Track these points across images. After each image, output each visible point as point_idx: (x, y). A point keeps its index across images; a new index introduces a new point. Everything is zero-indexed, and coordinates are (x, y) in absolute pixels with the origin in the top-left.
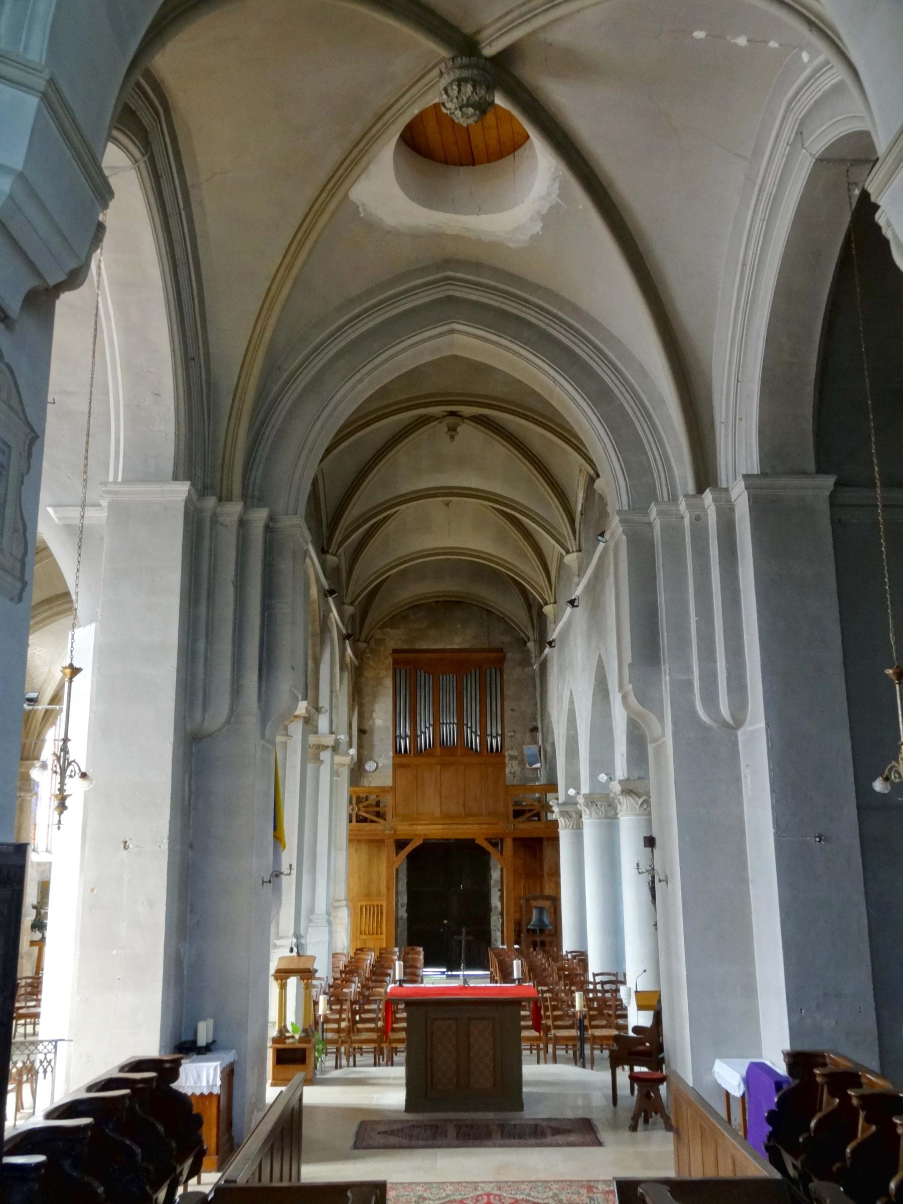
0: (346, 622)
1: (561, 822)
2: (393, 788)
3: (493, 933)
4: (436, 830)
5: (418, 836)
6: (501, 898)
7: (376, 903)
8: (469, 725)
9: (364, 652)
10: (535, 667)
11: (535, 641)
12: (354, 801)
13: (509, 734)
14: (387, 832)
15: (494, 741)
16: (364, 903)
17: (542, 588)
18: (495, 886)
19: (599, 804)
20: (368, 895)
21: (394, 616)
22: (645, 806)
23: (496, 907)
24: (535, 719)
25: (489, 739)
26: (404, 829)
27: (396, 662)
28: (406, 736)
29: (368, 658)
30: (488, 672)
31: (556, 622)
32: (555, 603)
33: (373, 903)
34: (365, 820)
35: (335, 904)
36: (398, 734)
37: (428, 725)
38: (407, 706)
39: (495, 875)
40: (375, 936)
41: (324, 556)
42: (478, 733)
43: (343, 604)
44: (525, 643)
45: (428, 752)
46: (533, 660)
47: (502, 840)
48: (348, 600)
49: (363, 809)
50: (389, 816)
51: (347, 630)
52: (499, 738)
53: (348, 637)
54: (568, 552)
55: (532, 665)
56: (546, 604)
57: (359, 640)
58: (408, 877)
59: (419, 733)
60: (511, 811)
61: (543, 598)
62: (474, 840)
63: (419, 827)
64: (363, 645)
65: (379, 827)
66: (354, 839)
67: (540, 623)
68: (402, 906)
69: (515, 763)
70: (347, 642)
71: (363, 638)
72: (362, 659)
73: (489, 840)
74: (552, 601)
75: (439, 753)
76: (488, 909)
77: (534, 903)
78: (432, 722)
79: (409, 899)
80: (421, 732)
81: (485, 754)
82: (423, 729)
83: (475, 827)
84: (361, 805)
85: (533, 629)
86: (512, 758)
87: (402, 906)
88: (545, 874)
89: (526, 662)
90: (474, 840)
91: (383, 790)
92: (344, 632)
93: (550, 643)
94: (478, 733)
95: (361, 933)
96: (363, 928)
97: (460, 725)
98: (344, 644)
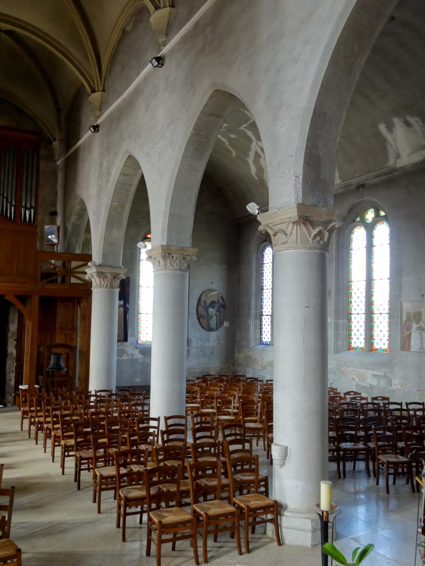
1: (96, 281)
3: (7, 375)
8: (5, 195)
10: (58, 163)
11: (61, 140)
18: (11, 337)
19: (175, 256)
22: (318, 239)
23: (12, 354)
24: (55, 206)
32: (104, 91)
39: (13, 328)
42: (13, 202)
46: (57, 157)
54: (157, 8)
55: (55, 161)
56: (93, 91)
60: (39, 274)
73: (17, 297)
74: (101, 88)
76: (4, 355)
77: (54, 350)
83: (5, 284)
88: (57, 327)
93: (96, 128)
94: (13, 202)
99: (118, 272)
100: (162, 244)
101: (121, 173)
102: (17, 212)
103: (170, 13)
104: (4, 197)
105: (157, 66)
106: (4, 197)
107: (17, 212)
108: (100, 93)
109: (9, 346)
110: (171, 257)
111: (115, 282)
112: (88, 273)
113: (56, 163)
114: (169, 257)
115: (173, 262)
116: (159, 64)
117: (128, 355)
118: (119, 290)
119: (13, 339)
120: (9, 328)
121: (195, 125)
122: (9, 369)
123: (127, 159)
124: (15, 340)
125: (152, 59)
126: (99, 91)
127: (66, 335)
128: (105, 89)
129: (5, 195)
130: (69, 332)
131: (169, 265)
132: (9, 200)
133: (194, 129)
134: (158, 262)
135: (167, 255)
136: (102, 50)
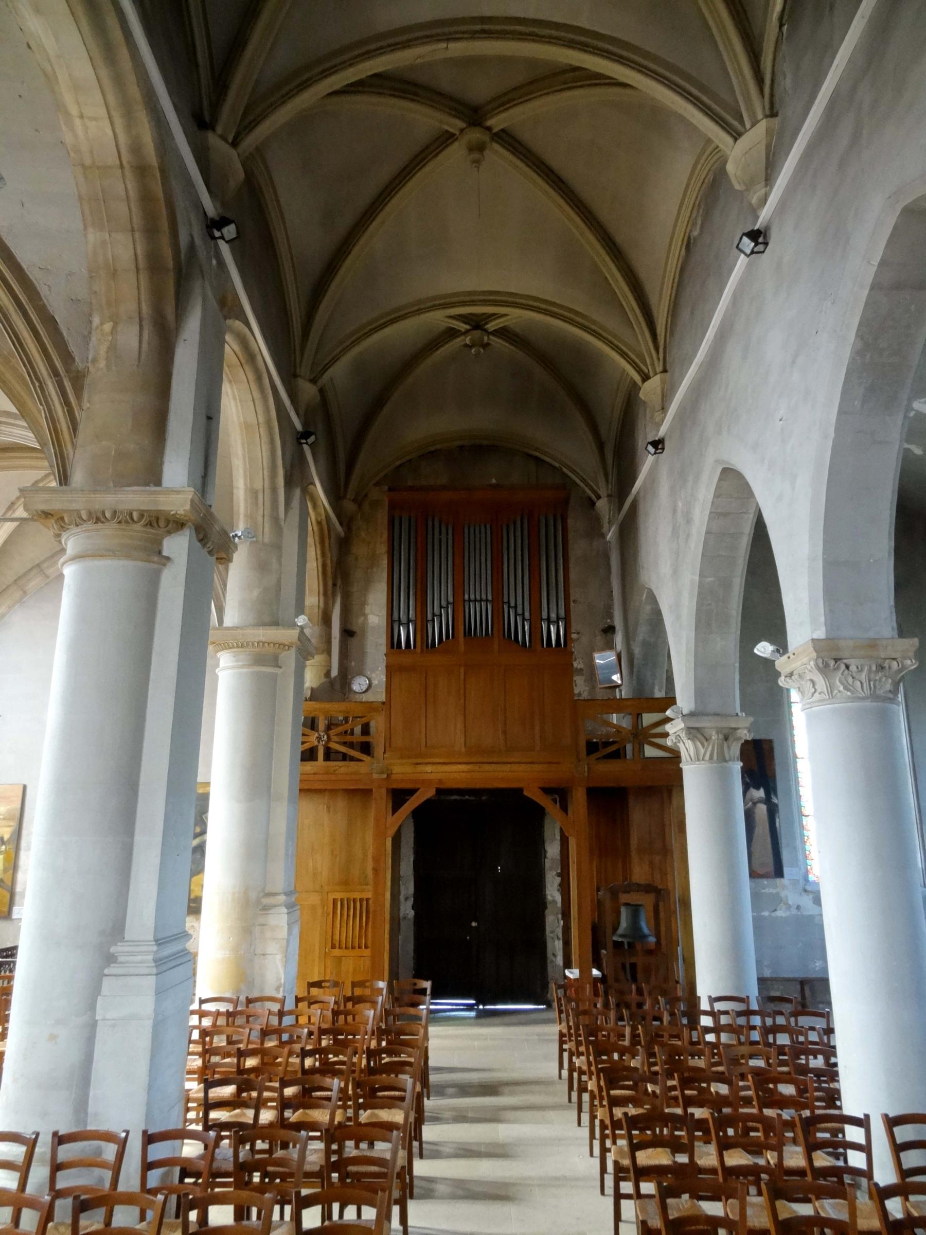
0: (302, 412)
1: (687, 749)
2: (387, 704)
4: (456, 773)
5: (427, 783)
6: (564, 888)
7: (358, 896)
8: (512, 604)
10: (608, 537)
11: (609, 496)
12: (322, 725)
14: (375, 776)
15: (553, 629)
16: (338, 896)
17: (640, 356)
18: (551, 869)
20: (345, 883)
23: (555, 902)
24: (610, 616)
25: (544, 625)
26: (403, 771)
28: (409, 621)
31: (664, 409)
32: (665, 371)
33: (353, 895)
34: (345, 757)
35: (266, 901)
36: (396, 617)
38: (412, 582)
39: (553, 850)
40: (357, 952)
42: (527, 615)
43: (295, 376)
44: (593, 504)
45: (446, 644)
49: (335, 739)
50: (379, 750)
53: (305, 435)
55: (603, 536)
56: (646, 378)
58: (416, 853)
59: (429, 617)
61: (639, 371)
62: (519, 791)
63: (429, 769)
68: (406, 899)
71: (350, 494)
73: (547, 791)
74: (659, 368)
75: (462, 648)
76: (541, 904)
77: (624, 898)
78: (451, 599)
80: (434, 615)
83: (523, 767)
84: (332, 733)
85: (606, 475)
87: (406, 899)
91: (371, 707)
92: (299, 426)
93: (658, 444)
94: (527, 615)
95: (333, 947)
96: (337, 937)
97: (498, 601)
99: (734, 726)
100: (815, 637)
101: (711, 513)
102: (535, 630)
103: (769, 132)
104: (509, 607)
105: (752, 252)
107: (535, 630)
108: (658, 377)
110: (843, 667)
111: (729, 748)
112: (671, 732)
114: (836, 669)
115: (850, 680)
116: (757, 244)
117: (789, 907)
118: (742, 764)
120: (545, 852)
121: (860, 325)
122: (552, 932)
123: (720, 479)
124: (559, 875)
125: (741, 239)
126: (656, 374)
127: (651, 863)
128: (668, 367)
130: (657, 859)
131: (841, 688)
132: (520, 611)
133: (860, 335)
134: (809, 684)
135: (832, 663)
136: (653, 300)
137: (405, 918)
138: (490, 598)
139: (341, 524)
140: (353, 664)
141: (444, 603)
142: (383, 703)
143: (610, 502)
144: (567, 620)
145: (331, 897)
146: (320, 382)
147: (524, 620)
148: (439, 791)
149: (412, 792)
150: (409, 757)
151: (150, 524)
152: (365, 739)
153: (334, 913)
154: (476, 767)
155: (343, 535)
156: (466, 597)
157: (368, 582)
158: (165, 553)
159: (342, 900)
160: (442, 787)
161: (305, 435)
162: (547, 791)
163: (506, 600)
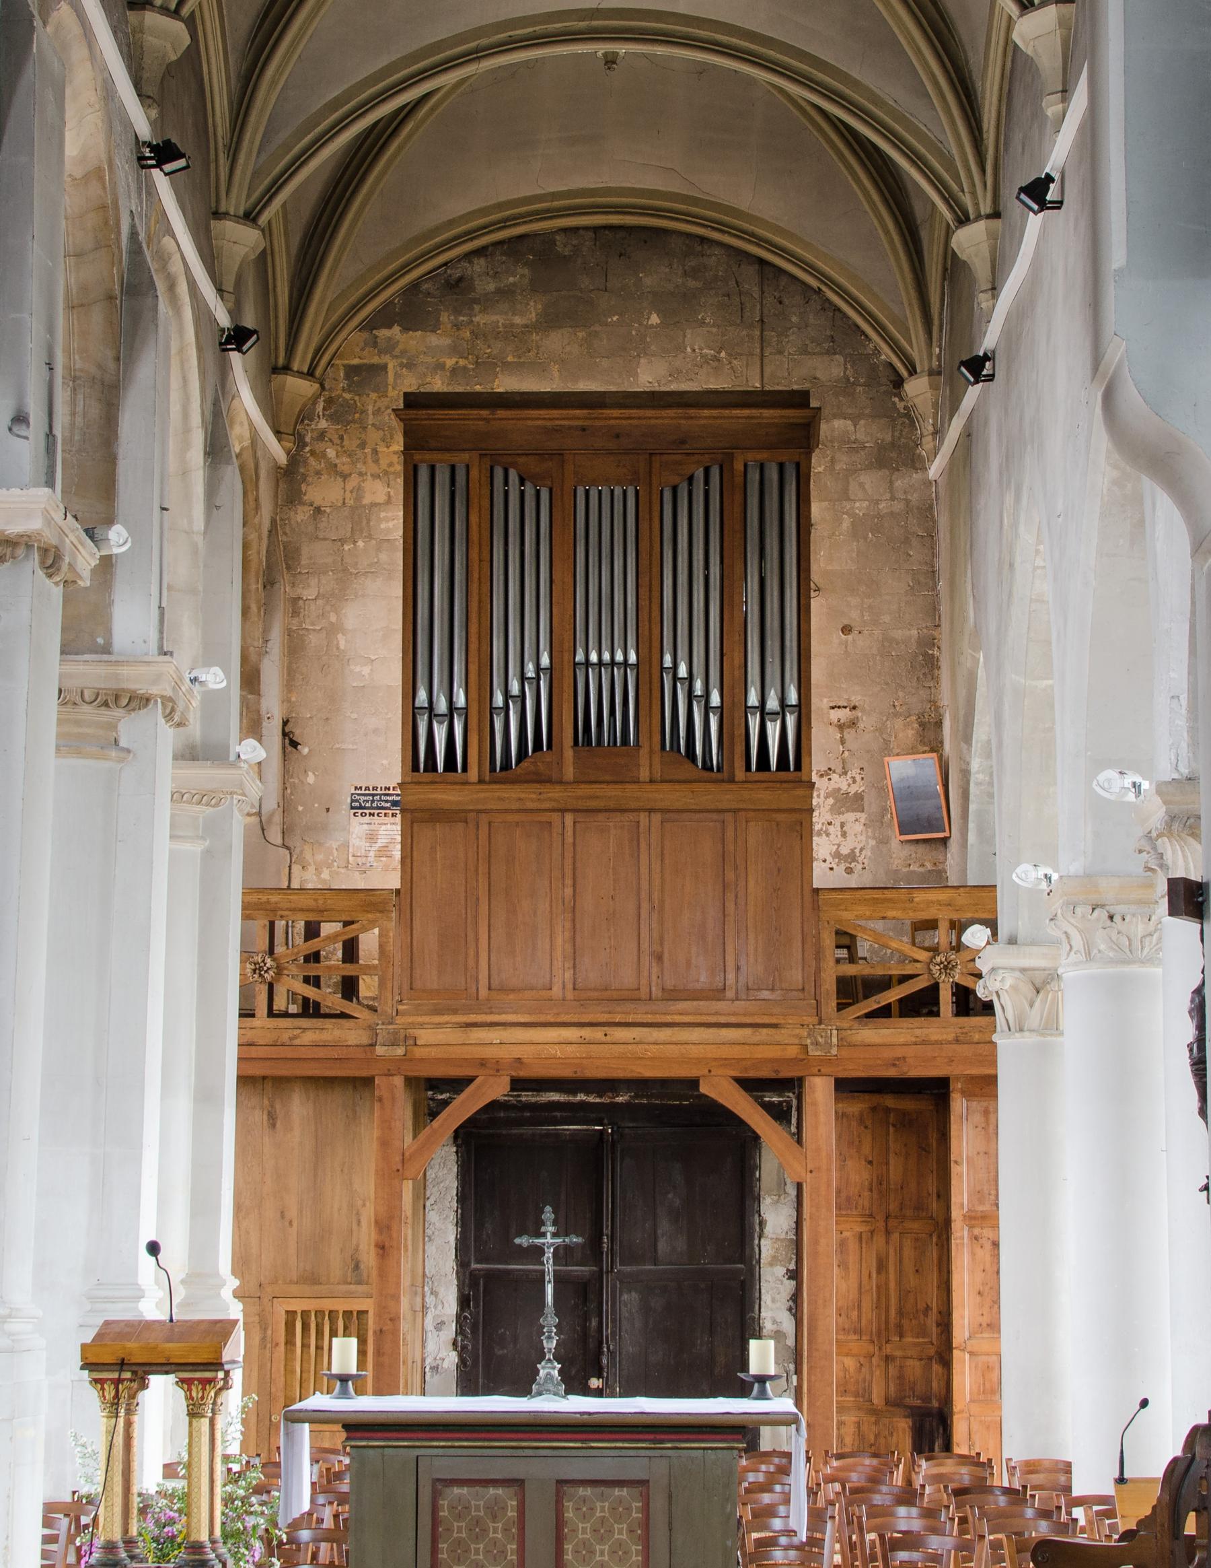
0: (229, 286)
2: (404, 897)
5: (495, 1066)
8: (683, 671)
9: (305, 415)
10: (935, 470)
13: (835, 715)
14: (380, 1050)
15: (773, 730)
16: (298, 1306)
18: (774, 1261)
21: (415, 286)
25: (754, 723)
26: (438, 1040)
27: (415, 443)
29: (322, 435)
30: (754, 476)
31: (994, 290)
32: (996, 215)
33: (327, 1305)
36: (422, 695)
37: (530, 673)
39: (775, 1219)
41: (132, 16)
42: (715, 699)
43: (217, 215)
44: (898, 383)
47: (794, 1085)
48: (236, 202)
51: (235, 312)
52: (791, 720)
53: (238, 337)
56: (963, 219)
57: (287, 369)
58: (463, 1222)
59: (499, 700)
60: (829, 985)
61: (951, 200)
62: (694, 1083)
64: (298, 388)
65: (350, 1035)
66: (261, 1081)
67: (945, 290)
68: (439, 1326)
69: (855, 823)
70: (235, 356)
72: (301, 443)
73: (750, 1085)
74: (986, 208)
75: (569, 772)
78: (545, 661)
79: (463, 1302)
81: (740, 774)
82: (515, 688)
86: (852, 802)
87: (439, 1326)
88: (956, 1214)
89: (901, 453)
90: (694, 1083)
92: (224, 320)
94: (715, 699)
98: (224, 370)
104: (675, 678)
106: (675, 678)
108: (981, 226)
109: (766, 1298)
113: (925, 469)
119: (780, 1271)
120: (762, 1224)
126: (979, 217)
129: (683, 671)
136: (974, 60)
137: (435, 1369)
138: (633, 658)
139: (278, 433)
140: (311, 779)
141: (530, 673)
142: (398, 892)
143: (934, 387)
144: (803, 711)
145: (281, 1308)
146: (263, 220)
147: (707, 709)
148: (518, 1084)
149: (458, 1084)
150: (455, 1012)
151: (106, 704)
152: (350, 970)
153: (290, 1342)
154: (597, 1034)
155: (282, 459)
156: (580, 657)
157: (346, 576)
158: (123, 743)
159: (305, 1314)
160: (523, 1074)
161: (238, 337)
162: (750, 1085)
163: (668, 661)
